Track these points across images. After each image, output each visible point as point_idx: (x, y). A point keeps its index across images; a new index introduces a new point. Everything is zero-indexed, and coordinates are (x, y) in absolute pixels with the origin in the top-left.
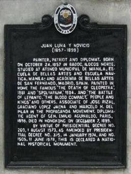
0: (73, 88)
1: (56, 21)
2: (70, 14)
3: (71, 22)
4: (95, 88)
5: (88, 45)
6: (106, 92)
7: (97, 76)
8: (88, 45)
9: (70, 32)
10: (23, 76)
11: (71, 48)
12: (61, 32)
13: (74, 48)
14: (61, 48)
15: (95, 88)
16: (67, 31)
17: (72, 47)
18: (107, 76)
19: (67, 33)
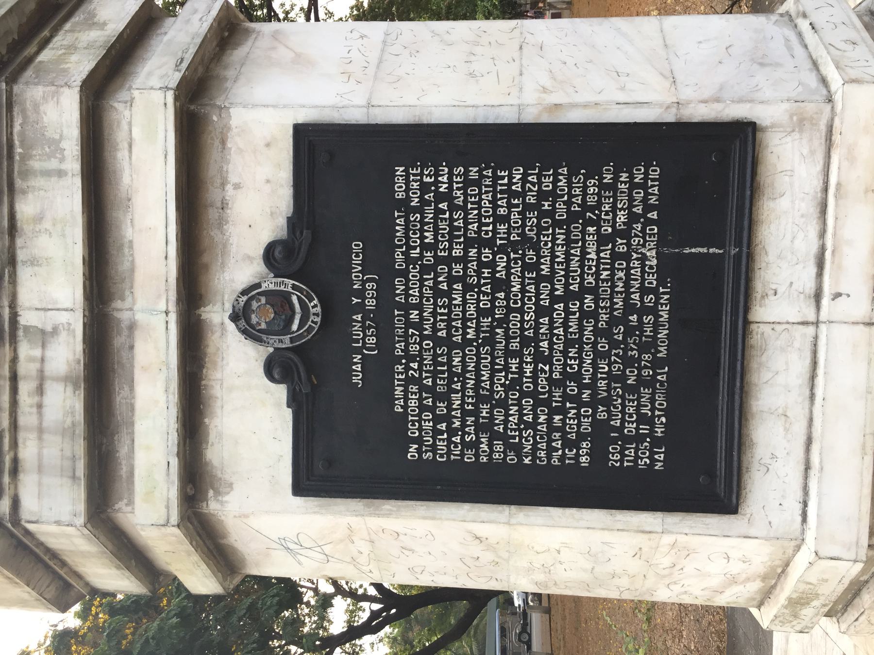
0: (485, 294)
1: (286, 342)
3: (285, 297)
4: (488, 225)
5: (357, 246)
6: (501, 192)
7: (451, 218)
8: (357, 246)
9: (316, 302)
10: (448, 446)
11: (364, 298)
12: (316, 327)
13: (364, 289)
14: (364, 328)
15: (488, 225)
16: (313, 311)
17: (361, 294)
18: (450, 188)
19: (318, 309)
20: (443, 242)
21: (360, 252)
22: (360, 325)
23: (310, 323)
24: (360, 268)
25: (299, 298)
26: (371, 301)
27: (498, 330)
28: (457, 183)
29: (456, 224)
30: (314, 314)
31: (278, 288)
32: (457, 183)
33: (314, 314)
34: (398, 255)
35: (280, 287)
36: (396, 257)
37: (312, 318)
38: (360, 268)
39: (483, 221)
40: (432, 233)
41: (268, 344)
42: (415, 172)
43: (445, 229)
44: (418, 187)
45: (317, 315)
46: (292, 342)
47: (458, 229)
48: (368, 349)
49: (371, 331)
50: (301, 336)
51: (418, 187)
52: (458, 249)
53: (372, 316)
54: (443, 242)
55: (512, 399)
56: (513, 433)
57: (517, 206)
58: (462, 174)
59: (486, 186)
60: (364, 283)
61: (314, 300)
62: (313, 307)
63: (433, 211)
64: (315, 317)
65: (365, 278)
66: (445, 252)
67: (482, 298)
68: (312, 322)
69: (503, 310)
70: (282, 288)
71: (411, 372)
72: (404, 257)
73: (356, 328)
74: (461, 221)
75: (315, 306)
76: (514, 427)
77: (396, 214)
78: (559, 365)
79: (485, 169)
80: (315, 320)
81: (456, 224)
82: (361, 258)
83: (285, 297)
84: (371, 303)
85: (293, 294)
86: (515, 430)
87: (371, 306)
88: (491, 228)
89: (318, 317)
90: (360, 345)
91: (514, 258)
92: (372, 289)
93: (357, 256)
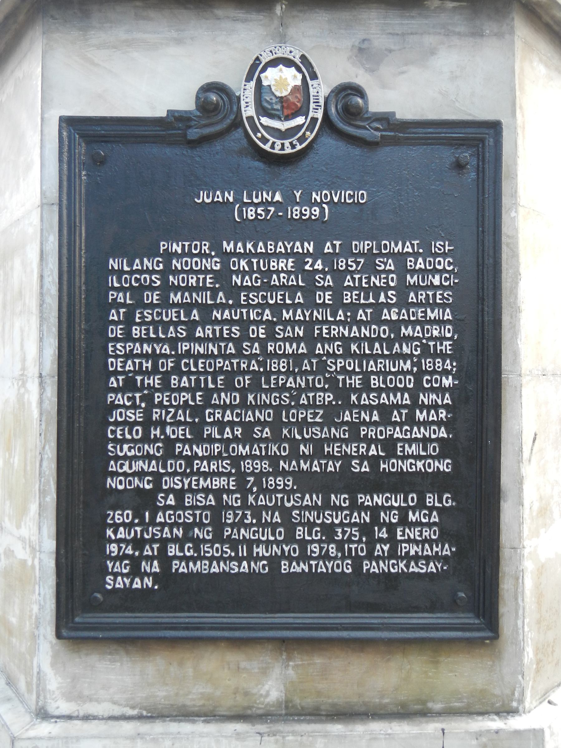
2: (299, 82)
4: (196, 365)
6: (198, 381)
9: (299, 147)
12: (267, 147)
13: (312, 204)
15: (196, 365)
16: (287, 143)
18: (217, 322)
20: (152, 314)
21: (354, 200)
22: (270, 200)
23: (272, 140)
24: (336, 200)
25: (300, 127)
26: (298, 213)
27: (409, 362)
28: (221, 331)
29: (172, 329)
30: (283, 144)
31: (312, 101)
32: (221, 331)
33: (283, 144)
34: (368, 245)
35: (314, 102)
36: (366, 242)
37: (279, 142)
38: (336, 200)
39: (200, 361)
40: (180, 302)
41: (244, 89)
42: (208, 280)
43: (167, 316)
44: (190, 285)
45: (283, 148)
46: (247, 118)
47: (165, 332)
48: (240, 212)
49: (263, 213)
50: (256, 130)
51: (190, 285)
52: (141, 331)
53: (280, 214)
54: (152, 314)
55: (314, 380)
56: (273, 381)
57: (194, 399)
58: (231, 337)
59: (238, 364)
60: (320, 205)
61: (300, 145)
62: (291, 143)
63: (204, 302)
64: (280, 146)
65: (324, 205)
66: (440, 299)
67: (119, 360)
68: (274, 143)
69: (430, 367)
70: (312, 105)
71: (310, 261)
72: (366, 252)
73: (265, 195)
74: (174, 335)
75: (293, 146)
76: (281, 382)
77: (415, 242)
78: (376, 434)
79: (257, 361)
80: (276, 146)
81: (172, 329)
82: (348, 201)
83: (303, 110)
84: (295, 213)
85: (306, 118)
86: (277, 383)
87: (292, 213)
88: (193, 369)
89: (280, 150)
90: (245, 200)
91: (134, 398)
92: (311, 214)
93: (350, 196)
